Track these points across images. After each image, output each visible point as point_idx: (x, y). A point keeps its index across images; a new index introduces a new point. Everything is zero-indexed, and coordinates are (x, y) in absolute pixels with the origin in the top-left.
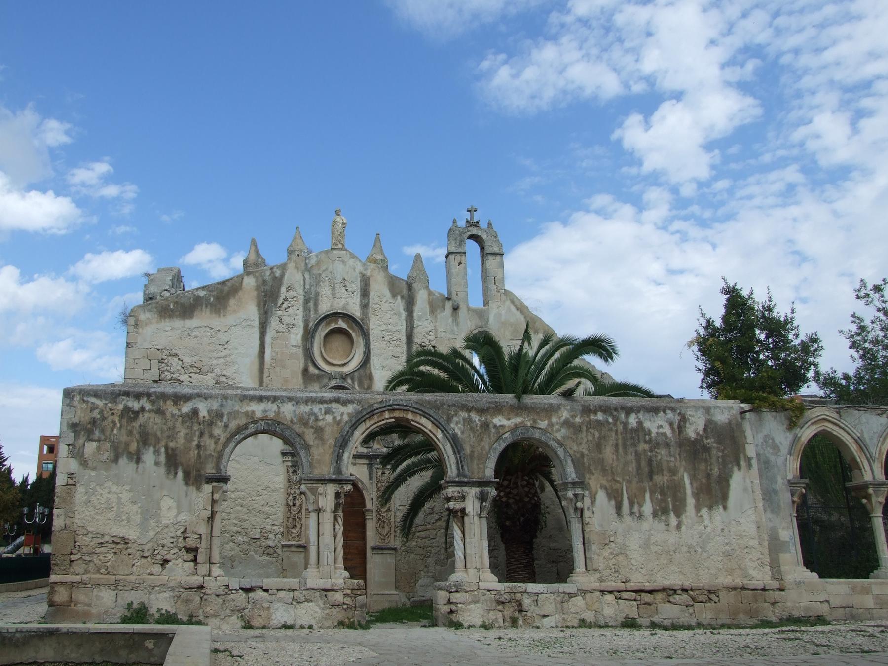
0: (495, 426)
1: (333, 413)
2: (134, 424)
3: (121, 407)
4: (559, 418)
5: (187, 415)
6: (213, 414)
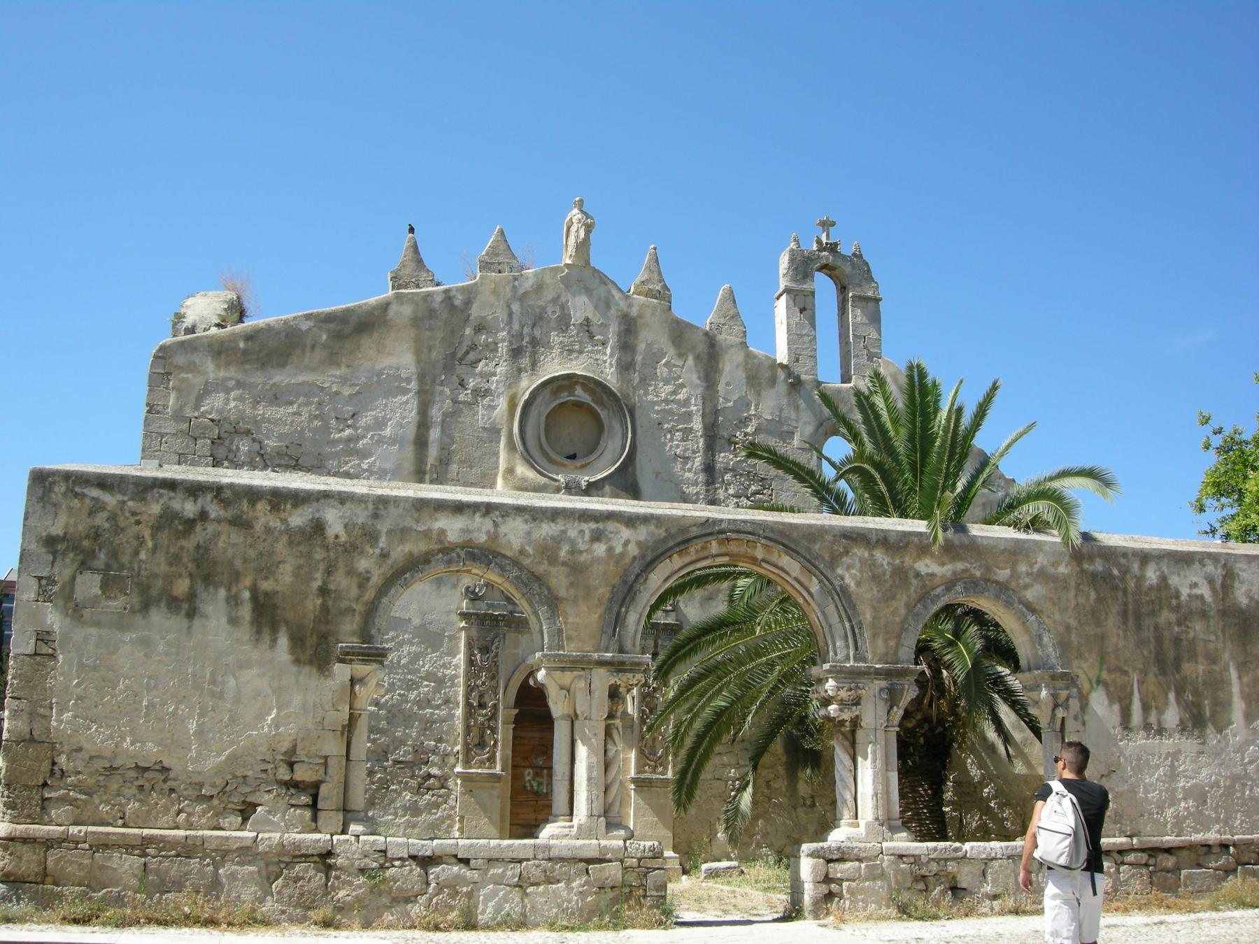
0: (918, 575)
1: (610, 539)
2: (184, 543)
3: (156, 509)
4: (1031, 566)
5: (301, 531)
6: (358, 532)
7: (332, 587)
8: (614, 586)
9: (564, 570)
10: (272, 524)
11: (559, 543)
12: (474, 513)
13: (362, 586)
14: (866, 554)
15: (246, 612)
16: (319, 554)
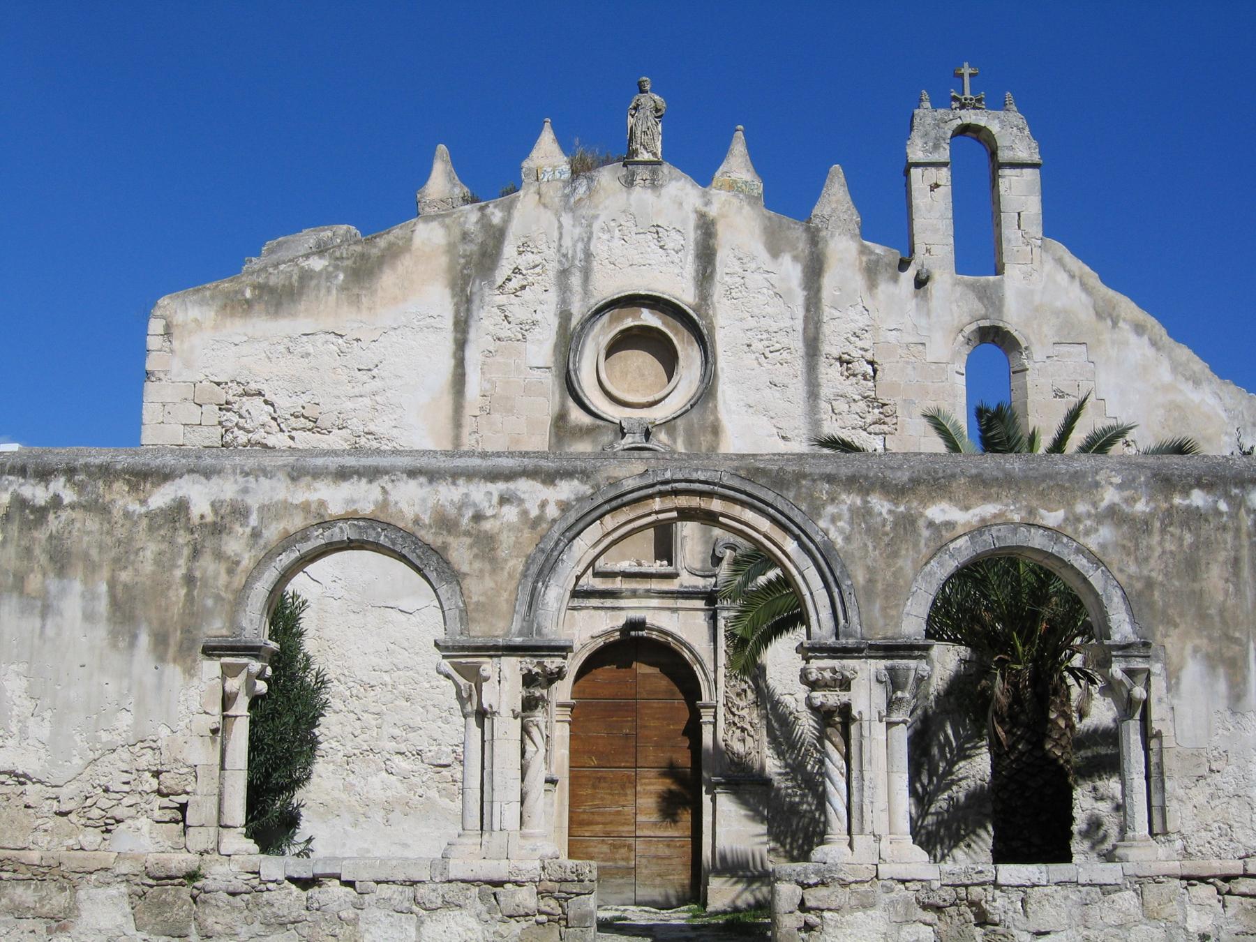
0: (931, 524)
1: (521, 501)
2: (36, 534)
7: (198, 574)
8: (528, 557)
9: (468, 541)
10: (131, 508)
11: (460, 508)
12: (360, 479)
13: (230, 572)
14: (858, 502)
15: (103, 606)
16: (182, 538)
